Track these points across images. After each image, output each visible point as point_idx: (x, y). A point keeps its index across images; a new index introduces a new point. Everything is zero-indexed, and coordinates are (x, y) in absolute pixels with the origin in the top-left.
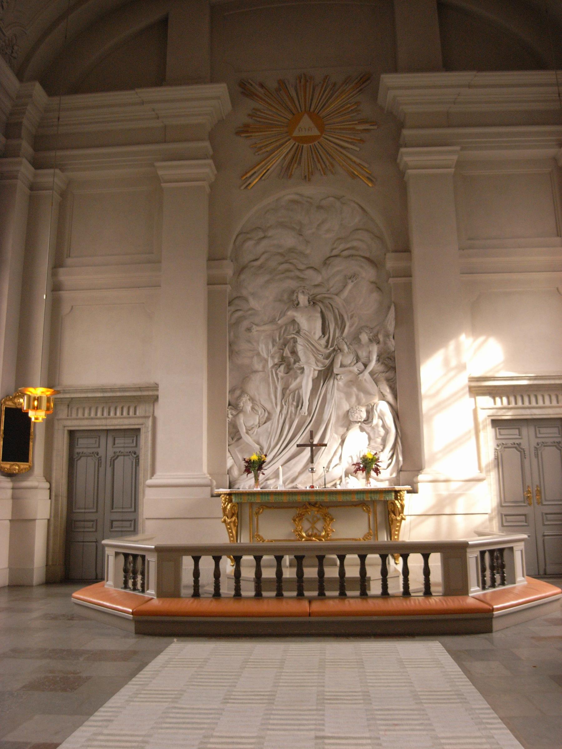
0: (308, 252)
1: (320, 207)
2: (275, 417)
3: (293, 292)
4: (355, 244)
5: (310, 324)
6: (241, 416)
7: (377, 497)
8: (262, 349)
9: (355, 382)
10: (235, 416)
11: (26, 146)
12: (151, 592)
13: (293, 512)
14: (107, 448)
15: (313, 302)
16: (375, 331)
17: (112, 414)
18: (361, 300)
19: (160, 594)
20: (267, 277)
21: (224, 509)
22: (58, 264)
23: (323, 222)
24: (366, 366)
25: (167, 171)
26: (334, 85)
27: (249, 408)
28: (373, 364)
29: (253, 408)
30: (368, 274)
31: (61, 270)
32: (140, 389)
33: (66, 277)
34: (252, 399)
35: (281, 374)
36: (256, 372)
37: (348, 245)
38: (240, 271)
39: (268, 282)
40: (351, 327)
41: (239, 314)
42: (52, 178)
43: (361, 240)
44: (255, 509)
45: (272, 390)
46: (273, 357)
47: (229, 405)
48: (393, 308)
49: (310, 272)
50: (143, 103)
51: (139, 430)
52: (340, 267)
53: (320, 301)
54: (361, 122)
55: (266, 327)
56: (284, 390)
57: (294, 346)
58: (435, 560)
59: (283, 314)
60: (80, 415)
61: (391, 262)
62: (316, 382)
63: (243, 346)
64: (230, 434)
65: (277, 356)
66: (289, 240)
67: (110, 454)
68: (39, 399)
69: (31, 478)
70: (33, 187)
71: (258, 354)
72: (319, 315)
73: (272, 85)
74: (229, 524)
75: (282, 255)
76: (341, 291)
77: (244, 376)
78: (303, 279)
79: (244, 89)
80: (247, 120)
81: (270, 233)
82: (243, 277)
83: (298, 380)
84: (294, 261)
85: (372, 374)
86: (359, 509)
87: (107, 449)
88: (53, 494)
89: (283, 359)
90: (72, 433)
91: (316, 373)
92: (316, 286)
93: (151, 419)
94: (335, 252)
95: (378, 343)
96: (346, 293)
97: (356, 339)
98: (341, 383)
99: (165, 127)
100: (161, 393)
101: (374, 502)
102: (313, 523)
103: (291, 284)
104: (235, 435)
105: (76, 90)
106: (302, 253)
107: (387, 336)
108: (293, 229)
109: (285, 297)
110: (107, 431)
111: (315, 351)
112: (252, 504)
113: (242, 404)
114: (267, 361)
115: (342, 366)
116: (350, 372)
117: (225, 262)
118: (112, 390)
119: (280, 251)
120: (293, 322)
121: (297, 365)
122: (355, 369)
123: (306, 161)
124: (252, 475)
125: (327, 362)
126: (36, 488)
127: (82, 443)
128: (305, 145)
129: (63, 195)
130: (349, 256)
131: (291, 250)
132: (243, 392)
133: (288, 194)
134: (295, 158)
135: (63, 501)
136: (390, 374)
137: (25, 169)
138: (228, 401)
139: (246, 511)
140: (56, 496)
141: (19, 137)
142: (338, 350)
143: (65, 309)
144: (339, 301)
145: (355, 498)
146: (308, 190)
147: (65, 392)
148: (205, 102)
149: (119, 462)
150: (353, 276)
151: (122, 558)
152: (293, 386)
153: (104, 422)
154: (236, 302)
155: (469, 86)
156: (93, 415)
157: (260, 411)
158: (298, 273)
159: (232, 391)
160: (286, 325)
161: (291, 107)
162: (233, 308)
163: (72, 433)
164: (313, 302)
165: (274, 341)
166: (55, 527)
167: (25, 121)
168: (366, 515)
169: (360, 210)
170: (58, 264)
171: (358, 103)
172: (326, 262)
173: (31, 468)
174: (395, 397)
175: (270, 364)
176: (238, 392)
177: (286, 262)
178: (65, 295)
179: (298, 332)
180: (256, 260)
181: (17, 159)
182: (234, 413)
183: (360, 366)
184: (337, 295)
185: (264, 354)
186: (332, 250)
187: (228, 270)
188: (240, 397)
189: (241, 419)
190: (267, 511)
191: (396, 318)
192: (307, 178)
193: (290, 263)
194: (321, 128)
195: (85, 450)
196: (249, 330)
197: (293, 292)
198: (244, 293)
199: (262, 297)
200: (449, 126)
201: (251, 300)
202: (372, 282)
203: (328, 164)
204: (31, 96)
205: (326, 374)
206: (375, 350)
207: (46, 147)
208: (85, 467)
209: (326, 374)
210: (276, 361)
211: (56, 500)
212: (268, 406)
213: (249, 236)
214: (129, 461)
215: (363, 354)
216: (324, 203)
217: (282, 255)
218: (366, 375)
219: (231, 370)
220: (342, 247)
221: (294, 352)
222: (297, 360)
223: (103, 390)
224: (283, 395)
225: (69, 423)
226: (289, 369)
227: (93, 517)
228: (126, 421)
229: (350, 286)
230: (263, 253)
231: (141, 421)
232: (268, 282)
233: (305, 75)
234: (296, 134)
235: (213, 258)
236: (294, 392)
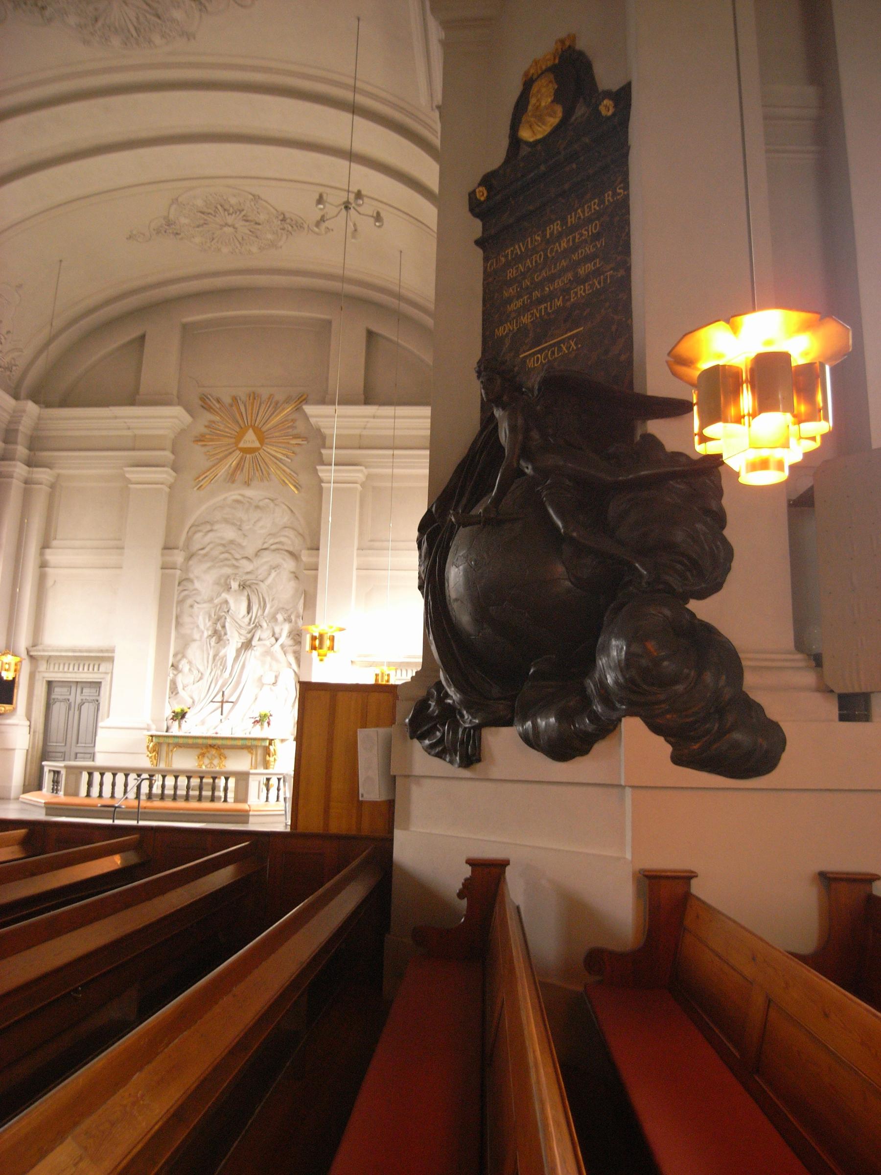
0: (244, 544)
1: (257, 507)
4: (283, 539)
5: (238, 606)
6: (180, 675)
7: (255, 743)
9: (268, 653)
10: (175, 675)
11: (21, 450)
12: (61, 793)
13: (199, 751)
14: (76, 696)
15: (243, 586)
16: (289, 612)
17: (81, 669)
18: (281, 586)
19: (66, 794)
20: (209, 564)
21: (148, 747)
23: (258, 520)
24: (277, 640)
25: (135, 474)
26: (277, 403)
28: (283, 639)
29: (190, 670)
30: (289, 565)
31: (48, 551)
32: (102, 651)
33: (51, 556)
34: (190, 663)
35: (213, 643)
36: (194, 640)
37: (276, 541)
38: (190, 557)
39: (209, 568)
40: (271, 607)
41: (186, 593)
42: (43, 475)
43: (287, 537)
44: (171, 748)
45: (205, 656)
46: (208, 630)
47: (172, 666)
49: (244, 562)
50: (116, 418)
51: (100, 683)
52: (268, 558)
53: (250, 586)
54: (296, 437)
55: (205, 605)
57: (224, 623)
58: (232, 782)
59: (219, 595)
60: (56, 669)
61: (305, 557)
62: (239, 652)
63: (186, 619)
64: (171, 688)
65: (211, 628)
66: (229, 533)
67: (78, 701)
68: (9, 664)
69: (14, 717)
70: (27, 482)
71: (198, 627)
73: (227, 400)
74: (151, 758)
75: (224, 545)
76: (266, 578)
77: (185, 643)
78: (237, 567)
80: (205, 430)
81: (216, 527)
82: (191, 562)
84: (233, 552)
85: (282, 646)
86: (245, 752)
87: (74, 699)
88: (32, 730)
89: (215, 632)
90: (49, 683)
91: (239, 645)
92: (248, 573)
93: (109, 675)
94: (265, 546)
96: (269, 580)
97: (274, 618)
99: (135, 436)
100: (117, 655)
101: (256, 746)
102: (211, 759)
103: (228, 571)
104: (174, 690)
105: (64, 403)
106: (239, 545)
107: (298, 616)
108: (233, 524)
109: (222, 581)
110: (77, 682)
112: (169, 744)
113: (180, 666)
114: (203, 632)
115: (260, 640)
116: (264, 645)
117: (176, 551)
118: (80, 651)
119: (223, 542)
120: (226, 602)
121: (225, 638)
122: (268, 643)
123: (250, 468)
124: (177, 722)
125: (249, 636)
126: (17, 725)
127: (58, 692)
128: (248, 456)
129: (53, 486)
130: (274, 550)
131: (232, 542)
132: (184, 656)
133: (234, 494)
134: (239, 467)
135: (40, 737)
136: (296, 648)
137: (20, 470)
139: (164, 749)
140: (34, 732)
141: (15, 443)
142: (258, 626)
143: (50, 582)
144: (263, 587)
145: (240, 743)
146: (249, 493)
147: (44, 651)
148: (166, 420)
149: (84, 708)
150: (276, 567)
151: (52, 773)
152: (221, 654)
153: (73, 675)
154: (185, 583)
155: (374, 417)
156: (66, 669)
157: (195, 672)
158: (234, 562)
159: (175, 655)
160: (221, 604)
161: (240, 422)
162: (181, 588)
163: (49, 683)
164: (243, 586)
165: (210, 616)
166: (32, 756)
167: (21, 428)
168: (250, 755)
169: (289, 512)
170: (45, 545)
171: (294, 421)
172: (257, 555)
173: (14, 710)
174: (299, 666)
175: (206, 634)
176: (180, 656)
177: (227, 552)
178: (49, 570)
181: (14, 462)
182: (175, 672)
183: (273, 640)
185: (202, 627)
186: (264, 543)
188: (180, 660)
190: (180, 750)
192: (247, 484)
193: (230, 553)
194: (262, 441)
195: (59, 697)
196: (192, 606)
197: (229, 577)
198: (191, 576)
199: (204, 581)
200: (360, 448)
201: (196, 582)
202: (293, 573)
203: (265, 472)
204: (24, 411)
205: (247, 645)
206: (286, 628)
207: (39, 449)
208: (58, 710)
209: (247, 645)
210: (210, 633)
211: (34, 736)
212: (202, 669)
213: (200, 528)
214: (92, 707)
215: (277, 630)
216: (261, 504)
217: (224, 545)
218: (277, 647)
219: (176, 638)
220: (272, 541)
221: (224, 627)
223: (74, 651)
224: (214, 659)
225: (46, 675)
226: (219, 640)
227: (62, 750)
228: (91, 676)
229: (273, 574)
231: (102, 676)
232: (209, 568)
233: (254, 393)
234: (241, 445)
235: (167, 547)
236: (222, 658)
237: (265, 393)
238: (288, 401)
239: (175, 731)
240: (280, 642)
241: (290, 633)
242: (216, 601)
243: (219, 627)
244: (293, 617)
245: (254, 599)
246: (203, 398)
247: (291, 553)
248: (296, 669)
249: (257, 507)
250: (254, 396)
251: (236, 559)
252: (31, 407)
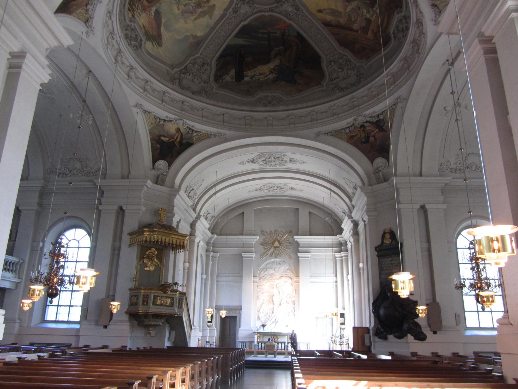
1: (279, 264)
54: (290, 243)
73: (269, 232)
79: (262, 233)
133: (272, 260)
146: (276, 259)
237: (279, 230)
238: (287, 232)
239: (262, 330)
246: (262, 231)
247: (290, 278)
250: (276, 231)
252: (215, 236)
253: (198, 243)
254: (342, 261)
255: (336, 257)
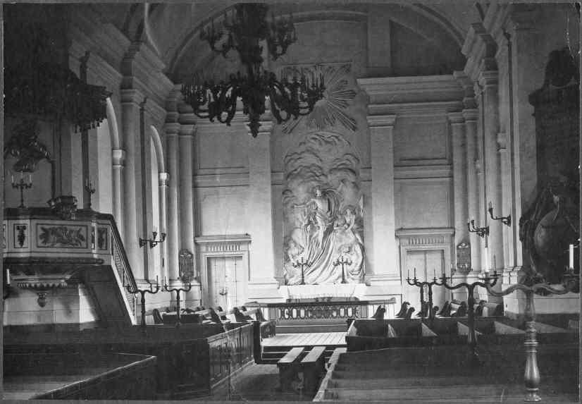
1: (327, 142)
2: (306, 250)
3: (314, 188)
5: (321, 205)
8: (299, 216)
15: (324, 193)
20: (301, 180)
22: (195, 175)
24: (349, 225)
27: (293, 245)
28: (353, 225)
33: (199, 180)
36: (297, 228)
42: (189, 129)
46: (305, 222)
48: (362, 198)
49: (322, 177)
56: (311, 236)
70: (180, 134)
72: (327, 201)
83: (317, 233)
85: (352, 229)
89: (310, 222)
95: (355, 214)
98: (337, 234)
100: (253, 239)
111: (325, 219)
120: (314, 203)
132: (291, 239)
138: (283, 243)
142: (336, 218)
154: (287, 192)
159: (285, 238)
162: (285, 196)
163: (209, 259)
172: (331, 171)
174: (363, 240)
175: (303, 225)
176: (288, 238)
179: (317, 209)
180: (296, 170)
183: (346, 226)
184: (335, 189)
187: (281, 177)
189: (289, 252)
191: (364, 203)
196: (293, 207)
197: (314, 188)
199: (300, 191)
205: (329, 231)
209: (329, 231)
215: (348, 220)
217: (309, 168)
221: (315, 219)
222: (316, 223)
224: (310, 239)
230: (300, 166)
232: (302, 182)
240: (350, 227)
241: (355, 220)
242: (308, 204)
243: (311, 219)
244: (357, 211)
245: (332, 201)
247: (352, 170)
248: (360, 241)
249: (327, 142)
251: (318, 176)
253: (142, 104)
254: (464, 129)
255: (450, 123)
